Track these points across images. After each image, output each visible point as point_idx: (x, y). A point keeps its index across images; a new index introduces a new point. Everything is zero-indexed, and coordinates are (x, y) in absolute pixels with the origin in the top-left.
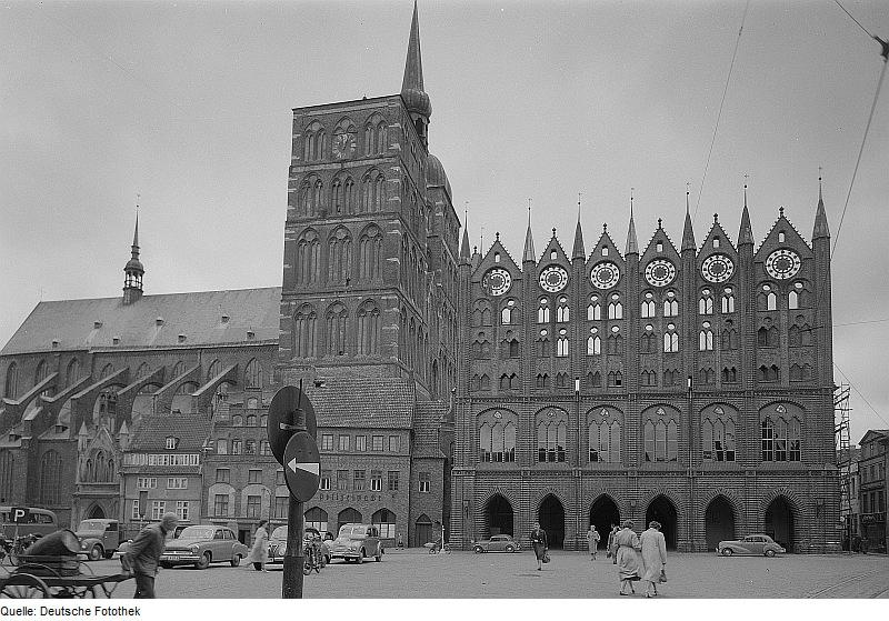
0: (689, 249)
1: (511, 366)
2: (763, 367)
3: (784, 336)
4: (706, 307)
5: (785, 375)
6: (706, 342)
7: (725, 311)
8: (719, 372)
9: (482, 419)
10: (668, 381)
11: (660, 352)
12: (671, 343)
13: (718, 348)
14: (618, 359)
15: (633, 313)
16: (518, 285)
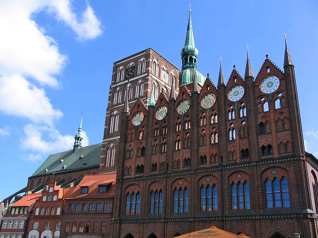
0: (221, 85)
1: (141, 162)
2: (263, 146)
3: (273, 125)
4: (231, 116)
5: (275, 149)
6: (233, 135)
7: (241, 116)
8: (238, 152)
9: (127, 191)
10: (213, 160)
11: (208, 144)
12: (215, 139)
13: (238, 138)
14: (188, 151)
15: (196, 125)
16: (146, 118)
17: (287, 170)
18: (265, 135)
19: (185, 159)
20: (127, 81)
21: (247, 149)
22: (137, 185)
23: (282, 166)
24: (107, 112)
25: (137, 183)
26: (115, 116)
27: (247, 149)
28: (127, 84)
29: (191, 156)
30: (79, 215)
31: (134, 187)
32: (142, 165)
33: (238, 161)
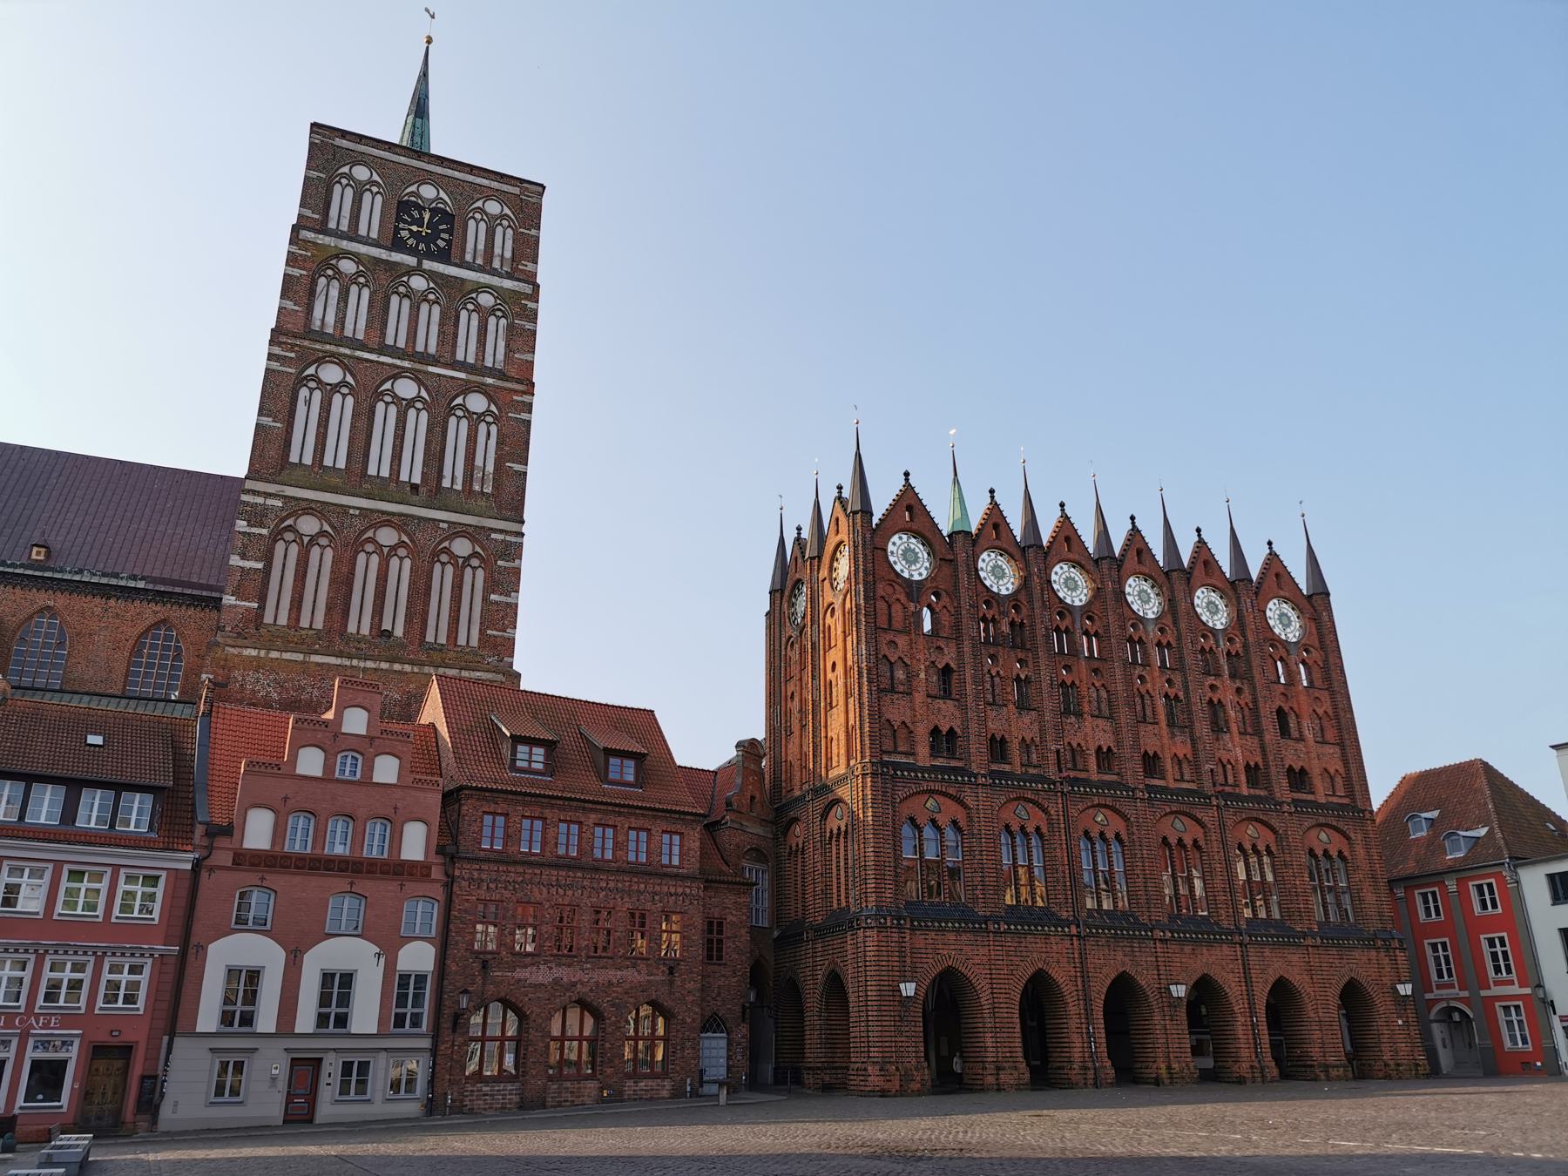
8: (1241, 767)
17: (1348, 838)
18: (1290, 742)
19: (1100, 748)
20: (411, 261)
21: (1256, 764)
22: (951, 797)
23: (1341, 825)
24: (277, 350)
25: (951, 791)
26: (330, 390)
27: (1256, 764)
28: (410, 271)
29: (1118, 743)
30: (546, 872)
31: (931, 801)
32: (951, 729)
33: (1245, 792)
